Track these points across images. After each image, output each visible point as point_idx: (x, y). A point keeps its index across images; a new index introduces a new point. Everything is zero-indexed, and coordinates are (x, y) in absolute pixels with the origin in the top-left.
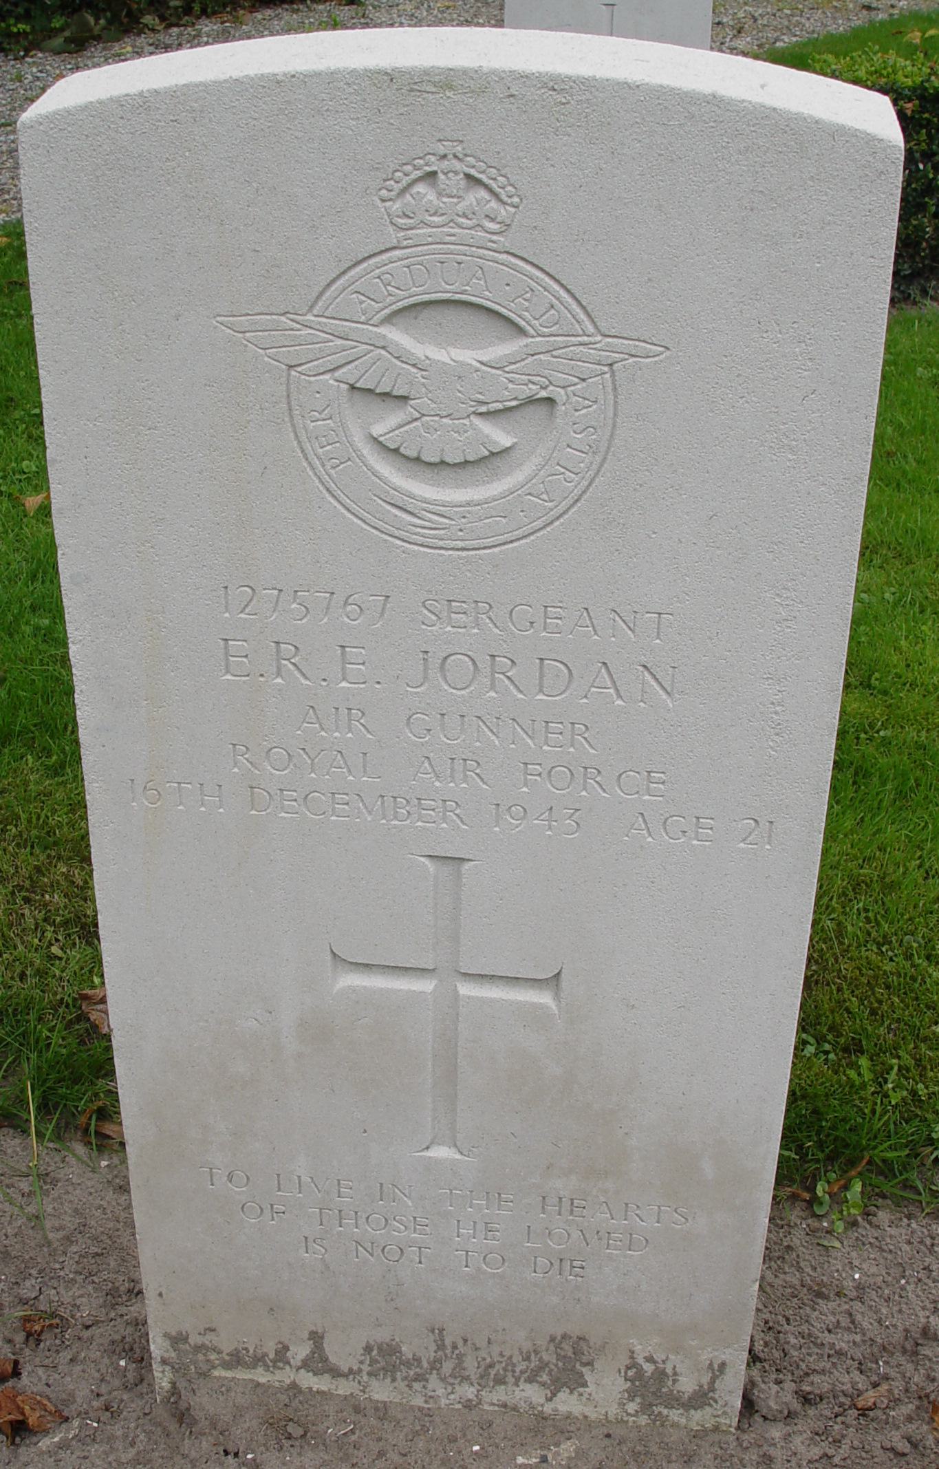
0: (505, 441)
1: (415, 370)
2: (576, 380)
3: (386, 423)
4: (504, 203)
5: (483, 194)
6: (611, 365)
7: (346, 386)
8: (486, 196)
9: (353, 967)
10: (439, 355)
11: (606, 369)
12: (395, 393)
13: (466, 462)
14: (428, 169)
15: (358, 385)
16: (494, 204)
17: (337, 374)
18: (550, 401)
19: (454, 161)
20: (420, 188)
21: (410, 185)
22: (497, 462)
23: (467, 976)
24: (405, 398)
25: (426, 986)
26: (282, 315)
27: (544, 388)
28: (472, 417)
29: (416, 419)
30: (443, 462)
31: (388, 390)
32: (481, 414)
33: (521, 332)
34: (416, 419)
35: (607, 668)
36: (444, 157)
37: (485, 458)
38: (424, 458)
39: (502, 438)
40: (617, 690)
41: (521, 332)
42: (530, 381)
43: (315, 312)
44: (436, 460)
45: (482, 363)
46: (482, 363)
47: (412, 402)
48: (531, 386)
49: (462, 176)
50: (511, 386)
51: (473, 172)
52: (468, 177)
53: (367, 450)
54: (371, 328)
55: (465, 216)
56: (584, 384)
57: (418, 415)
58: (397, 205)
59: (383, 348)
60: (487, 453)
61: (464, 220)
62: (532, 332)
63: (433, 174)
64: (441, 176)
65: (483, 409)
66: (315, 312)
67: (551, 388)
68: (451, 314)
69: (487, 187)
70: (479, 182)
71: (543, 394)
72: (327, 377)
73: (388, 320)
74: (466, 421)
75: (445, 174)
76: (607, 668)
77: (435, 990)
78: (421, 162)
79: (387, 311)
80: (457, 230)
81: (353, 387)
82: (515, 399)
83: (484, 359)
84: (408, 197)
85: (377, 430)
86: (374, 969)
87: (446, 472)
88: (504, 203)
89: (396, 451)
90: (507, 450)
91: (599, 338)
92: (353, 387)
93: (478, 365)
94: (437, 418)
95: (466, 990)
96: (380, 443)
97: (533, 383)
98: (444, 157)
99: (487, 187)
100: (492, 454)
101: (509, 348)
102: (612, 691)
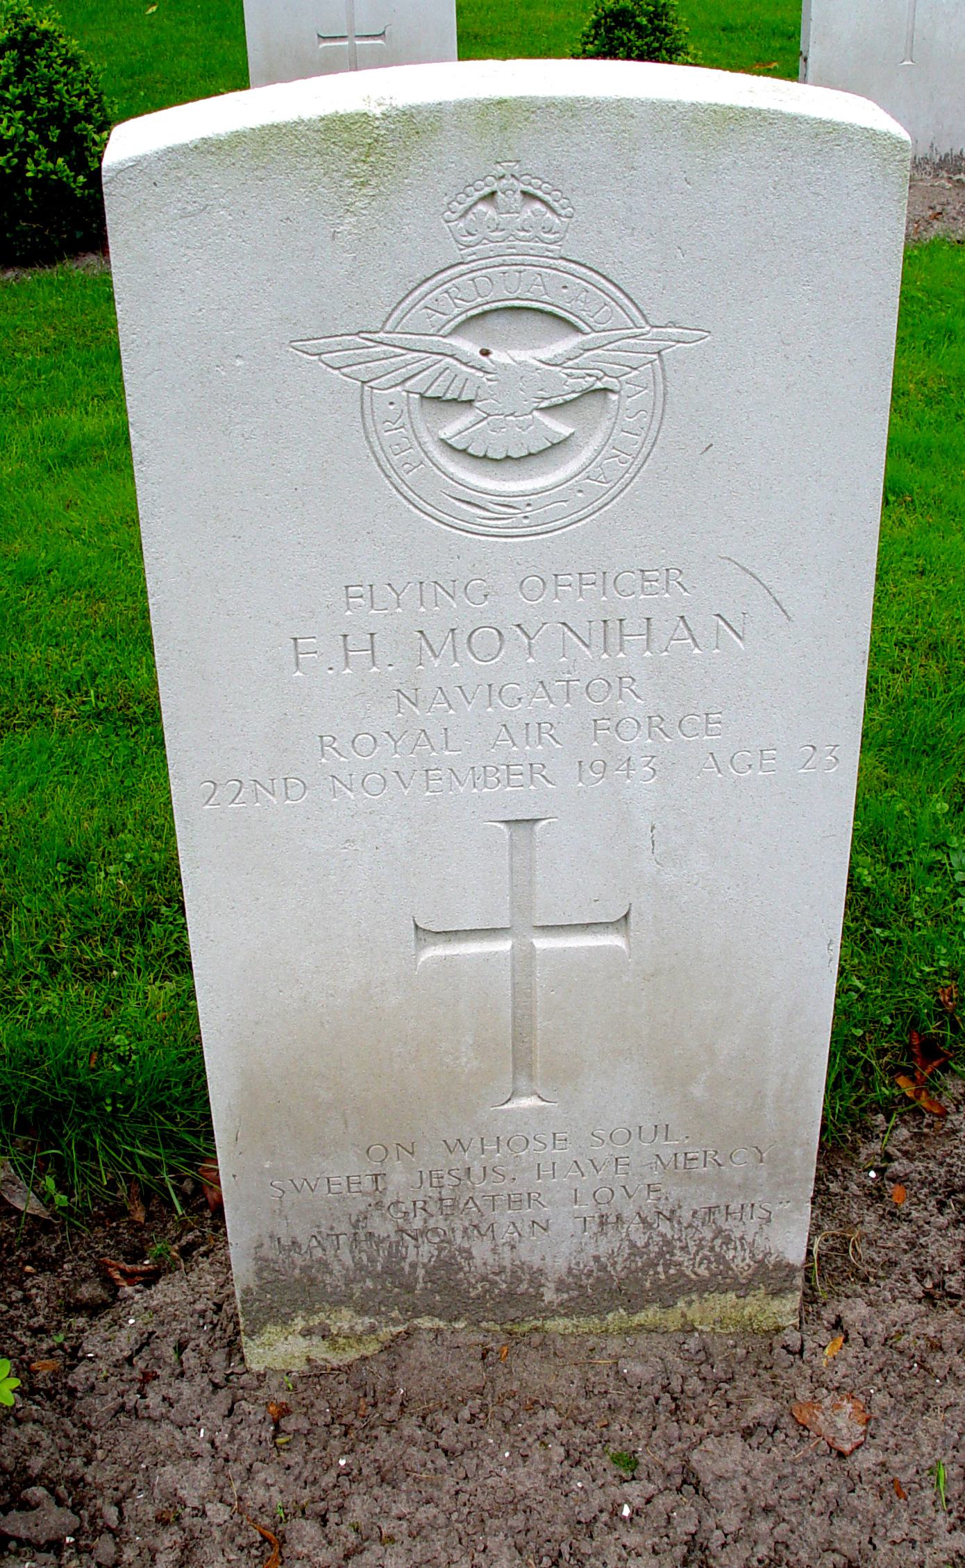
0: (565, 431)
1: (481, 374)
3: (455, 427)
5: (538, 206)
6: (659, 353)
7: (417, 396)
8: (544, 209)
9: (442, 937)
11: (655, 356)
12: (464, 398)
13: (530, 454)
14: (487, 190)
16: (549, 215)
18: (605, 390)
19: (512, 180)
20: (481, 207)
21: (471, 207)
22: (557, 453)
23: (546, 929)
24: (470, 402)
25: (503, 946)
26: (357, 334)
27: (599, 379)
28: (536, 413)
30: (508, 457)
32: (542, 409)
33: (577, 330)
35: (684, 621)
36: (503, 177)
38: (490, 455)
39: (560, 427)
40: (694, 640)
41: (577, 330)
45: (541, 361)
46: (541, 361)
48: (588, 379)
49: (518, 196)
50: (571, 381)
51: (530, 189)
52: (524, 193)
55: (524, 230)
56: (636, 372)
59: (451, 356)
61: (522, 234)
62: (588, 329)
63: (493, 193)
65: (545, 404)
66: (387, 328)
67: (606, 378)
71: (599, 385)
73: (455, 331)
76: (684, 621)
77: (513, 947)
78: (482, 183)
79: (453, 324)
80: (517, 243)
81: (422, 396)
82: (574, 392)
83: (543, 358)
84: (470, 216)
85: (447, 432)
86: (460, 934)
87: (534, 462)
88: (559, 215)
90: (566, 439)
91: (648, 328)
93: (538, 364)
95: (542, 943)
96: (450, 446)
97: (590, 376)
98: (503, 177)
101: (566, 344)
102: (690, 641)
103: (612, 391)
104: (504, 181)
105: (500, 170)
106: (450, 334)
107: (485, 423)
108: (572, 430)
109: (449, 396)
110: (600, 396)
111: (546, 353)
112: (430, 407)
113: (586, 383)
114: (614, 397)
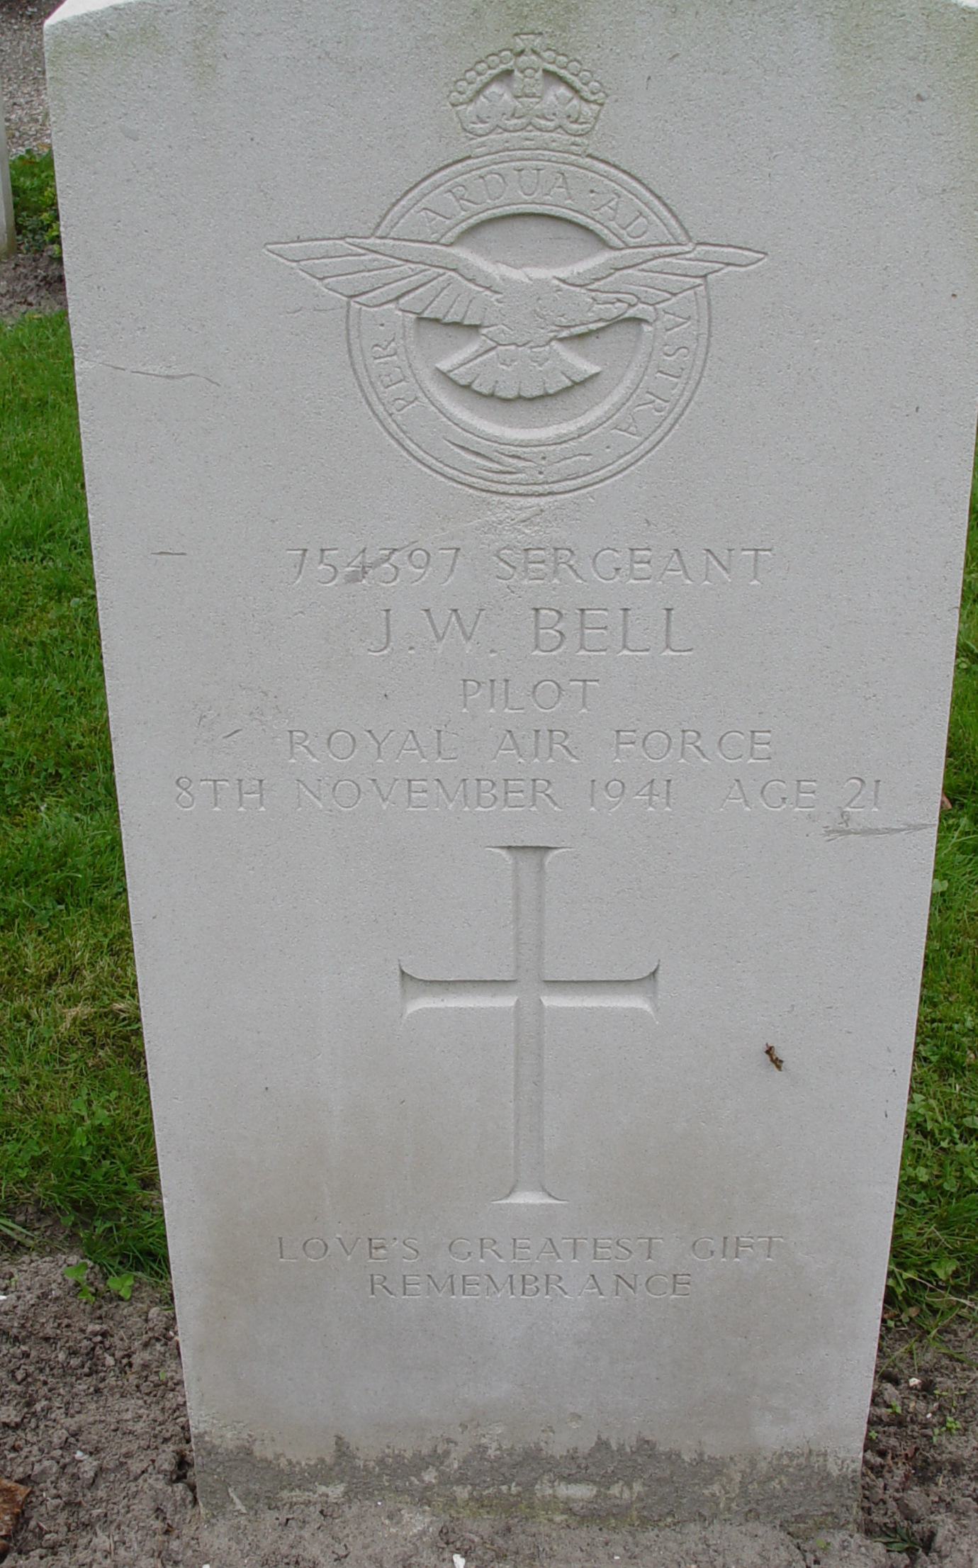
2: (668, 296)
4: (587, 101)
5: (562, 90)
6: (705, 276)
8: (569, 94)
10: (516, 275)
11: (698, 281)
12: (466, 323)
14: (503, 66)
15: (425, 315)
16: (575, 102)
17: (402, 301)
18: (638, 321)
19: (534, 57)
20: (494, 88)
24: (476, 327)
26: (341, 238)
27: (631, 306)
29: (493, 348)
31: (457, 319)
33: (605, 244)
34: (493, 348)
36: (522, 52)
37: (567, 389)
42: (619, 300)
43: (379, 233)
44: (511, 394)
45: (564, 281)
46: (564, 281)
47: (484, 331)
48: (618, 304)
49: (539, 74)
51: (552, 68)
52: (546, 72)
53: (433, 388)
54: (444, 248)
56: (674, 300)
57: (493, 344)
58: (470, 108)
60: (569, 384)
61: (543, 122)
62: (615, 242)
63: (509, 73)
64: (517, 73)
65: (565, 334)
67: (641, 306)
68: (533, 228)
69: (570, 86)
70: (562, 80)
71: (631, 313)
72: (391, 306)
74: (547, 348)
75: (522, 72)
81: (420, 319)
82: (601, 320)
83: (561, 276)
85: (444, 365)
88: (587, 101)
89: (467, 387)
92: (420, 319)
94: (513, 347)
96: (451, 379)
98: (522, 52)
99: (570, 86)
100: (575, 384)
103: (646, 321)
104: (523, 58)
105: (520, 44)
106: (451, 245)
107: (493, 353)
108: (595, 369)
109: (446, 320)
110: (632, 329)
111: (563, 273)
112: (432, 333)
113: (615, 311)
114: (646, 328)
